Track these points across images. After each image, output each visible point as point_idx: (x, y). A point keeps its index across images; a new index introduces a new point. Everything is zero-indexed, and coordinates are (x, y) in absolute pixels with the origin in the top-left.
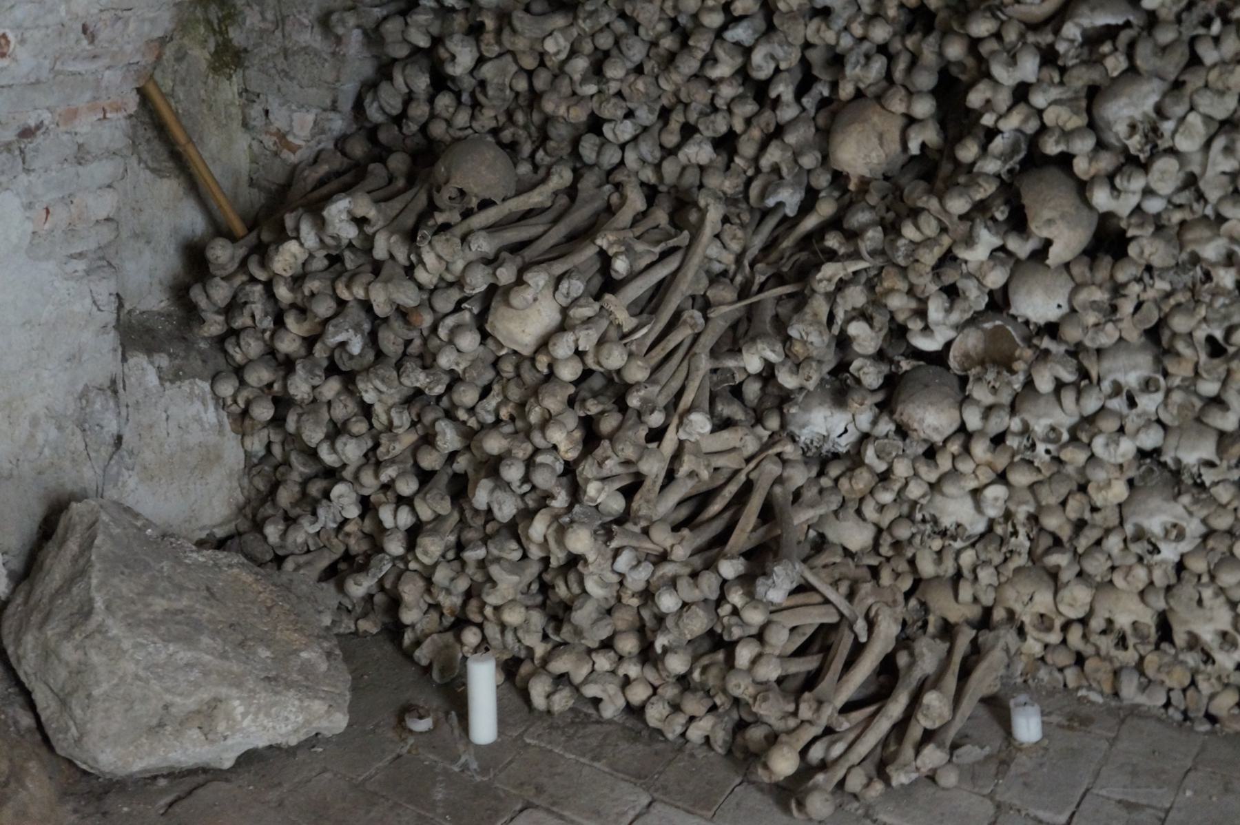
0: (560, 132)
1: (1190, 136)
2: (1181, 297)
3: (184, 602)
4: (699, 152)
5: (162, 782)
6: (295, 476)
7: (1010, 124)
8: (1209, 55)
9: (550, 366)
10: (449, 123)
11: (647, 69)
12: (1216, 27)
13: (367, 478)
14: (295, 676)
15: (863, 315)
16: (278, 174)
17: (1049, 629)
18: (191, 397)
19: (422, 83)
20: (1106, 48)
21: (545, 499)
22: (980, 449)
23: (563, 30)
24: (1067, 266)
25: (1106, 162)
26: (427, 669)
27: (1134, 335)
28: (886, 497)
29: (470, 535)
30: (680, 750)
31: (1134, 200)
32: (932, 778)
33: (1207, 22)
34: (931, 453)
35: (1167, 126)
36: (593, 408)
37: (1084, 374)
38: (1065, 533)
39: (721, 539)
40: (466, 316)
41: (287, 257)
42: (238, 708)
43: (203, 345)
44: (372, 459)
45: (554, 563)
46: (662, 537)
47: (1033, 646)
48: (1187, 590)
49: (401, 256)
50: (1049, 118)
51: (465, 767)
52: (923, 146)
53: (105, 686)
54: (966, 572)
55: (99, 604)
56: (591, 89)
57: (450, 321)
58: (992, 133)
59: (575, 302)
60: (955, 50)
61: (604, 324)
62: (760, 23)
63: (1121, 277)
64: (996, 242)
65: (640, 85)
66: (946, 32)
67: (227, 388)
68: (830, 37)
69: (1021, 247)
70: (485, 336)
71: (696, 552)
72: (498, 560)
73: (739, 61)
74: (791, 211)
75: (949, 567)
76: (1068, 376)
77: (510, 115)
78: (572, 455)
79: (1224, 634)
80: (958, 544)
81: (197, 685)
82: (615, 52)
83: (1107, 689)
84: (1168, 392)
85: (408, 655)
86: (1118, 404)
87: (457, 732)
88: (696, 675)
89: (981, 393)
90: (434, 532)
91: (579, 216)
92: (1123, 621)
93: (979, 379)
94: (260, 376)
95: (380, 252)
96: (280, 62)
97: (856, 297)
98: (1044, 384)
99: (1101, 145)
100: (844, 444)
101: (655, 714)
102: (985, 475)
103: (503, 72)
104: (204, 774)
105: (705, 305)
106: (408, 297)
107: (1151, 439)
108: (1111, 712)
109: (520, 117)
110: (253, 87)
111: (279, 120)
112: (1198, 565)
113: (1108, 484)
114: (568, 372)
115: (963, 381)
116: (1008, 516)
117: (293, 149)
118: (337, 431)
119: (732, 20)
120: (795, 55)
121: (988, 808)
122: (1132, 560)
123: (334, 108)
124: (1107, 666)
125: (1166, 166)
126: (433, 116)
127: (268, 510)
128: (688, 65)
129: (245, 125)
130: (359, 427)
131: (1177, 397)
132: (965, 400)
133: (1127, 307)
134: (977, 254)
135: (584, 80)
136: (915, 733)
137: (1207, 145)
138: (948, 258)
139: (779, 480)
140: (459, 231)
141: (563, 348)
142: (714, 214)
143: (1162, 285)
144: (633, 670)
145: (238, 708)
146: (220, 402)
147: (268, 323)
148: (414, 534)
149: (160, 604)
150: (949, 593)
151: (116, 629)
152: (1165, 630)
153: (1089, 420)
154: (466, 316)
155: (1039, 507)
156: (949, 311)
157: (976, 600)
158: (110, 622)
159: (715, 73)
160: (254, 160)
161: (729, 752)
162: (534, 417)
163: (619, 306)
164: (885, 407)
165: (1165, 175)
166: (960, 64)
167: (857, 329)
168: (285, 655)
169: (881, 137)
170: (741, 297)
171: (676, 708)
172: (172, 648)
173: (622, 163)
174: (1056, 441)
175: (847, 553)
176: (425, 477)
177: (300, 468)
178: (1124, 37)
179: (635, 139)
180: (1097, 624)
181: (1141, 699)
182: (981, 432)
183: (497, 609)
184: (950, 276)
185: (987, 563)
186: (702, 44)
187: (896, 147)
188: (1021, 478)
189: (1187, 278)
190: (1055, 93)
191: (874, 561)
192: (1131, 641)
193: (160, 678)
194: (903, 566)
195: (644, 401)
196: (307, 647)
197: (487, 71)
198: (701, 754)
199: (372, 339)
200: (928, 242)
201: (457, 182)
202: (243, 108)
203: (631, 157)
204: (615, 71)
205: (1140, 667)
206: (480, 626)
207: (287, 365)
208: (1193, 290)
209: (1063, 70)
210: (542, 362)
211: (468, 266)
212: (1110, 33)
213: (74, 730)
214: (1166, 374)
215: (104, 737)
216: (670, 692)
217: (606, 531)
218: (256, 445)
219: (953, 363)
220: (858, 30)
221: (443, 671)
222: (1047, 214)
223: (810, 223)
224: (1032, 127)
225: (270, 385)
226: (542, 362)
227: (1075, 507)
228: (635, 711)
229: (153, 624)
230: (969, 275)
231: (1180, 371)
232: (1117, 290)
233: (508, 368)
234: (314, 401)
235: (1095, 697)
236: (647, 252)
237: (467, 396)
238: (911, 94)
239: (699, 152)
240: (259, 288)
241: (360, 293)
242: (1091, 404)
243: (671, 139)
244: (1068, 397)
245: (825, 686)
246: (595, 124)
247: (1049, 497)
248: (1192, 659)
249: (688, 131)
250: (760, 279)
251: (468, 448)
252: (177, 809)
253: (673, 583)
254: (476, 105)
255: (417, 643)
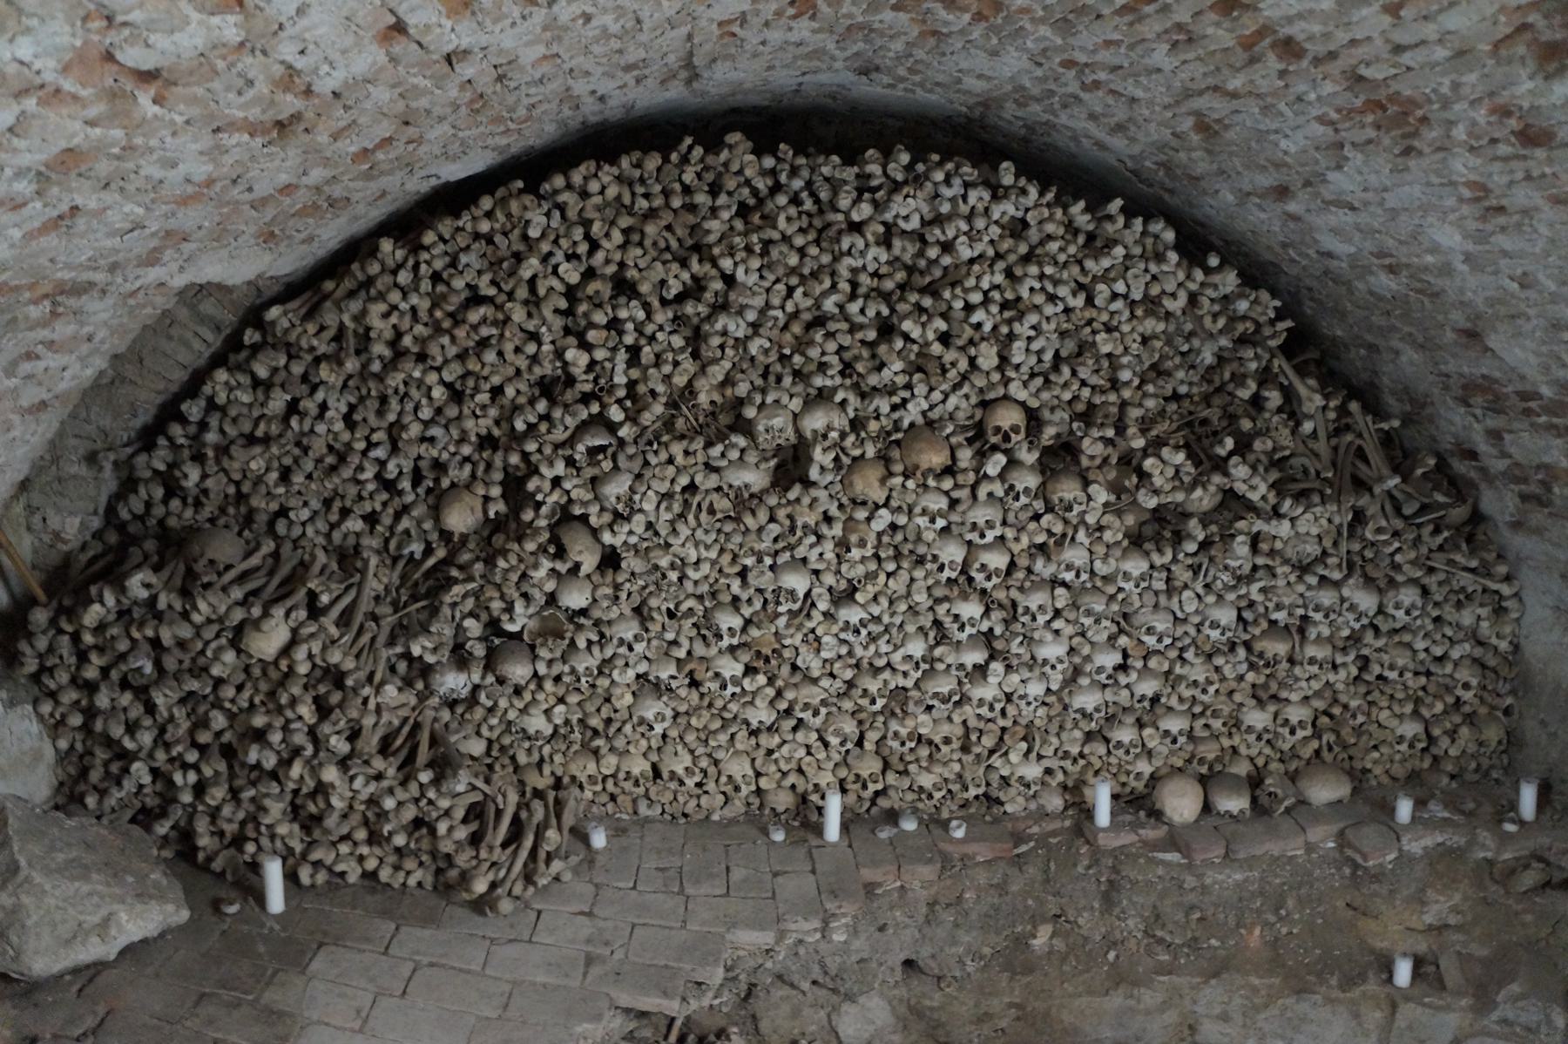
0: (262, 518)
1: (649, 502)
2: (652, 588)
3: (74, 854)
4: (355, 524)
5: (68, 978)
6: (98, 762)
7: (555, 497)
8: (653, 460)
9: (290, 667)
10: (179, 517)
11: (315, 476)
12: (655, 446)
13: (161, 756)
14: (152, 891)
15: (472, 614)
16: (54, 558)
17: (595, 783)
18: (23, 716)
19: (159, 492)
20: (601, 457)
21: (297, 752)
22: (549, 685)
23: (261, 455)
24: (588, 576)
25: (607, 518)
26: (222, 874)
27: (627, 611)
28: (494, 721)
29: (239, 782)
30: (404, 893)
31: (623, 537)
32: (557, 879)
33: (650, 443)
34: (518, 691)
35: (637, 497)
36: (322, 689)
37: (602, 635)
38: (600, 728)
39: (410, 760)
40: (223, 641)
41: (93, 614)
42: (124, 916)
43: (23, 681)
44: (161, 741)
45: (305, 790)
46: (379, 764)
47: (588, 794)
48: (669, 749)
49: (178, 606)
50: (574, 495)
51: (272, 929)
52: (497, 513)
53: (35, 918)
54: (547, 758)
55: (23, 862)
56: (281, 490)
57: (213, 645)
58: (538, 505)
59: (301, 624)
60: (514, 459)
61: (323, 636)
62: (389, 447)
63: (620, 580)
64: (550, 565)
65: (313, 486)
66: (507, 450)
67: (46, 708)
68: (435, 453)
69: (563, 567)
70: (239, 651)
71: (399, 769)
72: (267, 795)
73: (377, 469)
74: (418, 556)
75: (536, 757)
76: (595, 638)
77: (223, 510)
78: (313, 721)
79: (687, 769)
80: (540, 743)
81: (98, 906)
82: (294, 467)
83: (630, 811)
84: (649, 640)
85: (205, 868)
86: (623, 650)
87: (257, 909)
88: (412, 845)
89: (544, 653)
90: (216, 784)
91: (285, 570)
92: (636, 771)
93: (542, 645)
94: (69, 697)
95: (162, 603)
96: (56, 486)
97: (470, 604)
98: (582, 644)
99: (602, 509)
100: (465, 693)
101: (384, 875)
102: (552, 700)
103: (219, 482)
104: (99, 967)
105: (375, 618)
106: (186, 632)
107: (642, 668)
108: (634, 823)
109: (231, 510)
110: (35, 504)
111: (54, 522)
112: (674, 733)
113: (623, 695)
114: (303, 669)
115: (532, 647)
116: (567, 722)
117: (65, 542)
118: (132, 728)
119: (371, 445)
120: (412, 464)
121: (591, 888)
122: (638, 736)
123: (95, 513)
124: (629, 798)
125: (639, 519)
126: (168, 514)
127: (82, 787)
128: (347, 473)
129: (29, 529)
130: (147, 722)
131: (655, 643)
132: (535, 658)
133: (623, 596)
134: (540, 574)
135: (276, 485)
136: (542, 855)
137: (658, 507)
138: (524, 576)
139: (435, 720)
140: (218, 586)
141: (300, 654)
142: (374, 561)
143: (641, 582)
144: (365, 850)
145: (124, 916)
146: (40, 717)
147: (73, 660)
148: (200, 789)
149: (60, 857)
150: (536, 772)
151: (38, 878)
152: (657, 773)
153: (607, 662)
154: (223, 641)
155: (585, 714)
156: (527, 607)
157: (553, 773)
158: (34, 874)
159: (363, 477)
160: (35, 551)
161: (435, 888)
162: (284, 700)
163: (328, 621)
164: (490, 664)
165: (638, 524)
166: (517, 467)
167: (469, 623)
168: (142, 878)
169: (472, 510)
170: (396, 612)
171: (397, 868)
172: (77, 884)
173: (304, 534)
174: (591, 675)
175: (472, 758)
176: (203, 749)
177: (101, 755)
178: (610, 451)
179: (311, 519)
180: (622, 775)
181: (649, 813)
182: (547, 676)
183: (269, 827)
184: (525, 588)
185: (557, 751)
186: (355, 460)
187: (480, 515)
188: (573, 699)
189: (653, 578)
190: (576, 481)
191: (489, 761)
192: (642, 781)
193: (73, 905)
194: (507, 761)
195: (356, 681)
196: (153, 871)
197: (209, 483)
198: (418, 892)
199: (158, 664)
200: (512, 569)
201: (210, 554)
202: (27, 518)
203: (310, 531)
204: (298, 479)
205: (647, 796)
206: (256, 840)
207: (91, 688)
208: (657, 584)
209: (578, 470)
210: (284, 665)
211: (229, 609)
212: (602, 449)
213: (11, 952)
214: (647, 630)
215: (36, 953)
216: (392, 859)
217: (343, 763)
218: (63, 744)
219: (525, 637)
220: (452, 449)
221: (234, 874)
222: (578, 548)
223: (431, 562)
224: (564, 500)
225: (78, 702)
226: (284, 665)
227: (605, 712)
228: (371, 876)
229: (59, 871)
230: (534, 586)
231: (655, 628)
232: (617, 587)
233: (257, 672)
234: (114, 708)
235: (625, 817)
236: (337, 588)
237: (229, 692)
238: (486, 484)
239: (355, 524)
240: (66, 638)
241: (150, 633)
242: (609, 653)
243: (334, 517)
244: (596, 650)
245: (488, 838)
246: (283, 512)
247: (590, 708)
248: (673, 785)
249: (345, 513)
250: (404, 598)
251: (231, 726)
252: (87, 991)
253: (391, 791)
254: (198, 504)
255: (210, 859)
